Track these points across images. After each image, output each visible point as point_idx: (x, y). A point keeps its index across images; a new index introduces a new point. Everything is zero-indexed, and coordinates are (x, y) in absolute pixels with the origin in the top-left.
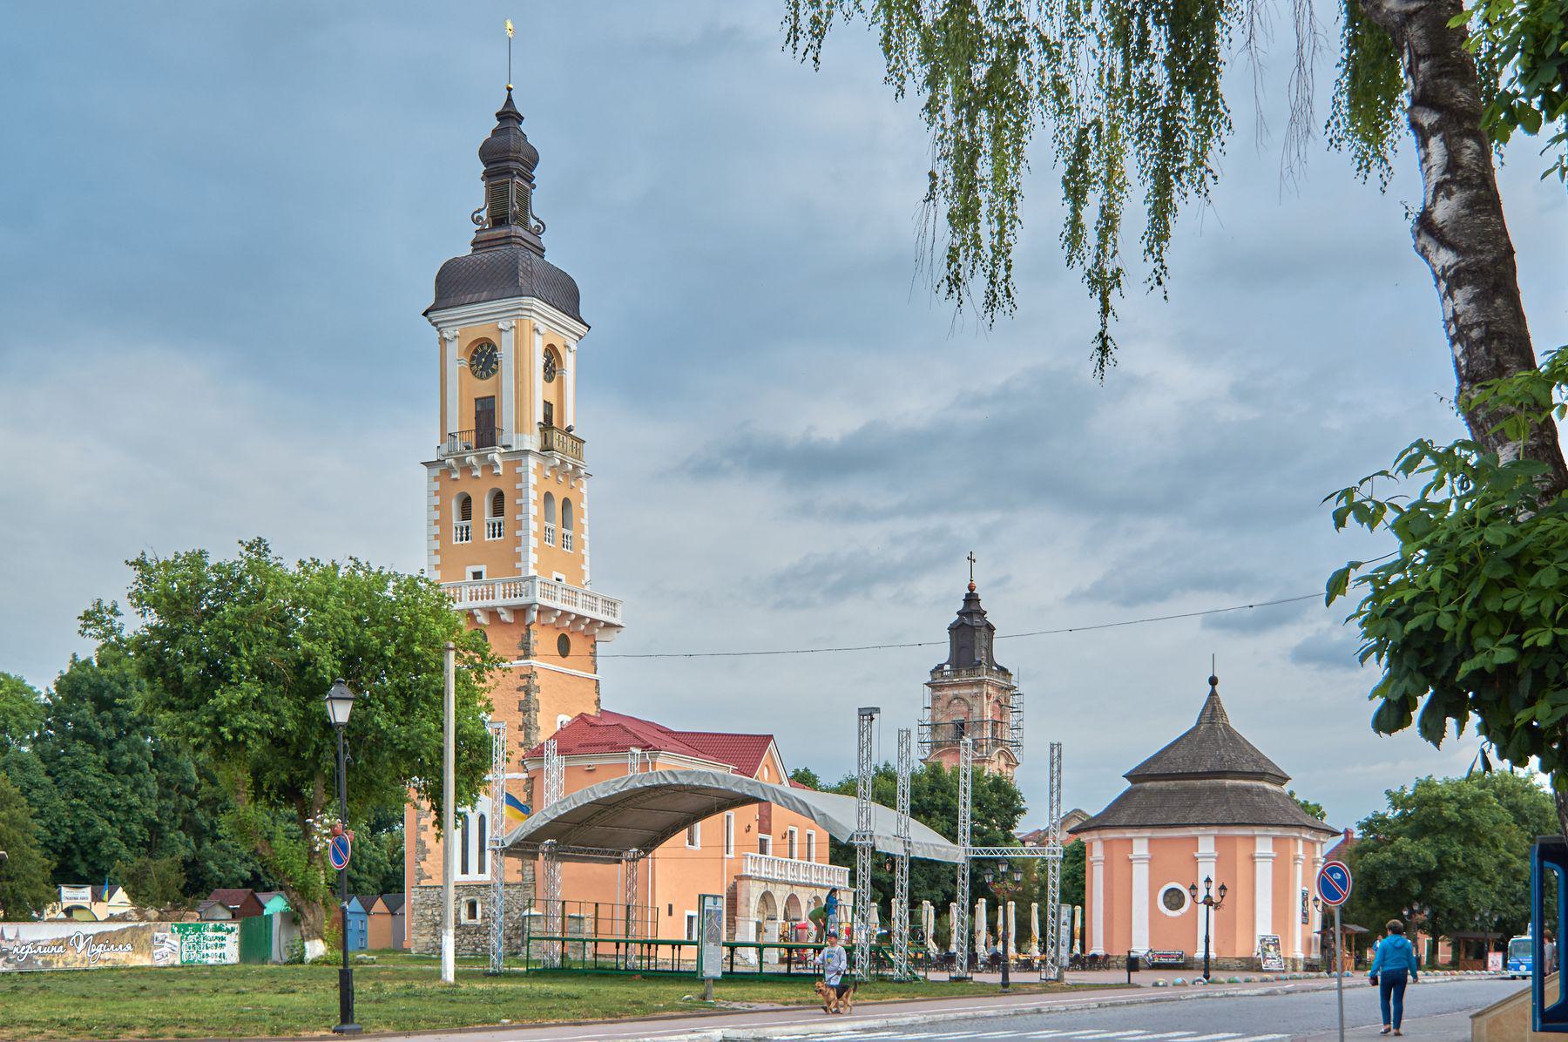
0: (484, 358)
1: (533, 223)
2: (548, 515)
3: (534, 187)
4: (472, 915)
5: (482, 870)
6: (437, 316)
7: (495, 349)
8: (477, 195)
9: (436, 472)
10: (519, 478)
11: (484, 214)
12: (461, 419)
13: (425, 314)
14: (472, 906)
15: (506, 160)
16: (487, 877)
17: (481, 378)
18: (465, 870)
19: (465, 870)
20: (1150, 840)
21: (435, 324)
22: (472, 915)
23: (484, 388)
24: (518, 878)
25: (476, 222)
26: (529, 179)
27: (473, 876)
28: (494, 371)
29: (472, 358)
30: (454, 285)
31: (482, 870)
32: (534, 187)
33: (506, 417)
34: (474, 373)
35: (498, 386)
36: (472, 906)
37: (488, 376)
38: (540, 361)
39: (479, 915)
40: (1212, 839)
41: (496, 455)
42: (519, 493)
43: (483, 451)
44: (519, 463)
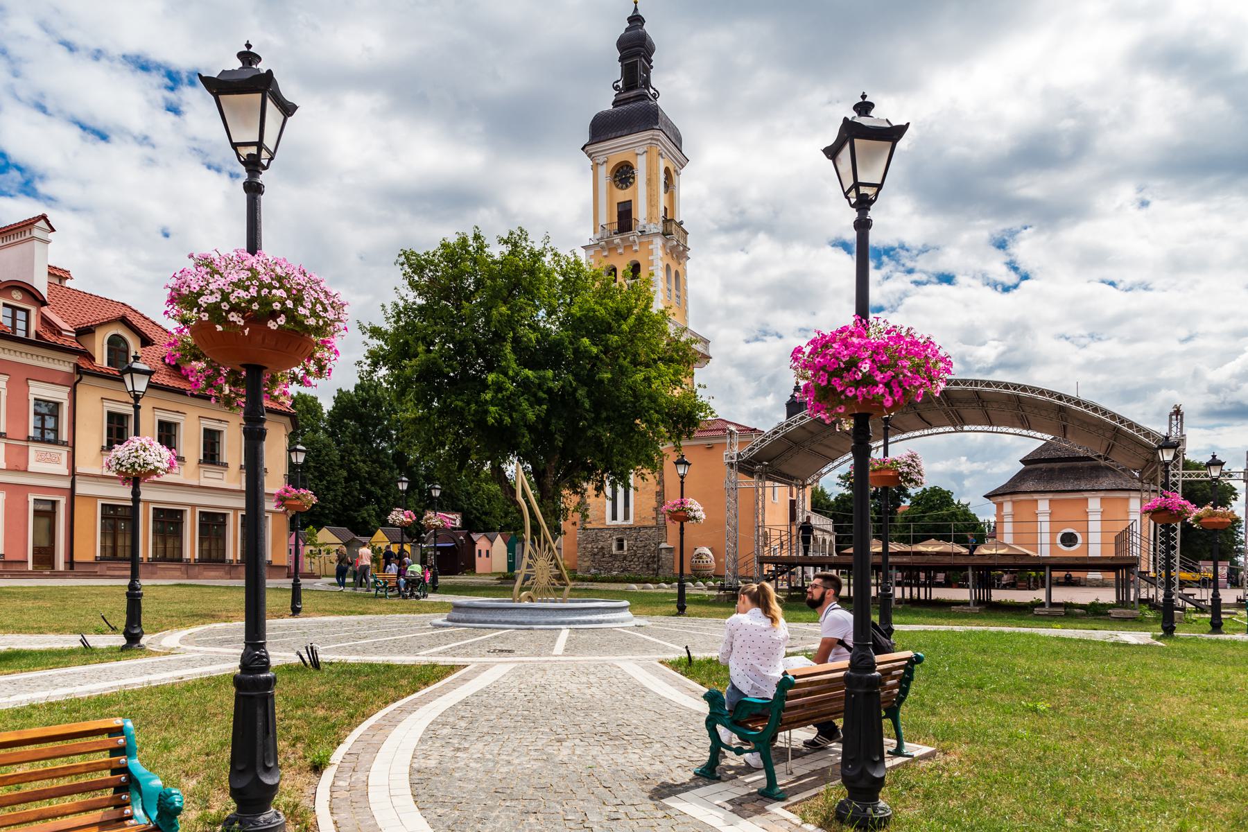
0: (623, 174)
1: (652, 91)
2: (668, 281)
4: (620, 547)
5: (626, 517)
7: (632, 168)
9: (591, 252)
10: (651, 252)
11: (620, 84)
12: (608, 216)
14: (620, 541)
15: (635, 50)
16: (631, 522)
18: (614, 517)
19: (614, 517)
20: (1050, 501)
21: (589, 156)
22: (620, 547)
23: (622, 195)
25: (615, 88)
26: (650, 61)
27: (620, 520)
30: (603, 128)
31: (626, 517)
33: (641, 213)
35: (635, 193)
36: (620, 541)
38: (662, 176)
39: (626, 548)
40: (1098, 500)
41: (632, 236)
42: (651, 263)
43: (626, 235)
44: (651, 243)
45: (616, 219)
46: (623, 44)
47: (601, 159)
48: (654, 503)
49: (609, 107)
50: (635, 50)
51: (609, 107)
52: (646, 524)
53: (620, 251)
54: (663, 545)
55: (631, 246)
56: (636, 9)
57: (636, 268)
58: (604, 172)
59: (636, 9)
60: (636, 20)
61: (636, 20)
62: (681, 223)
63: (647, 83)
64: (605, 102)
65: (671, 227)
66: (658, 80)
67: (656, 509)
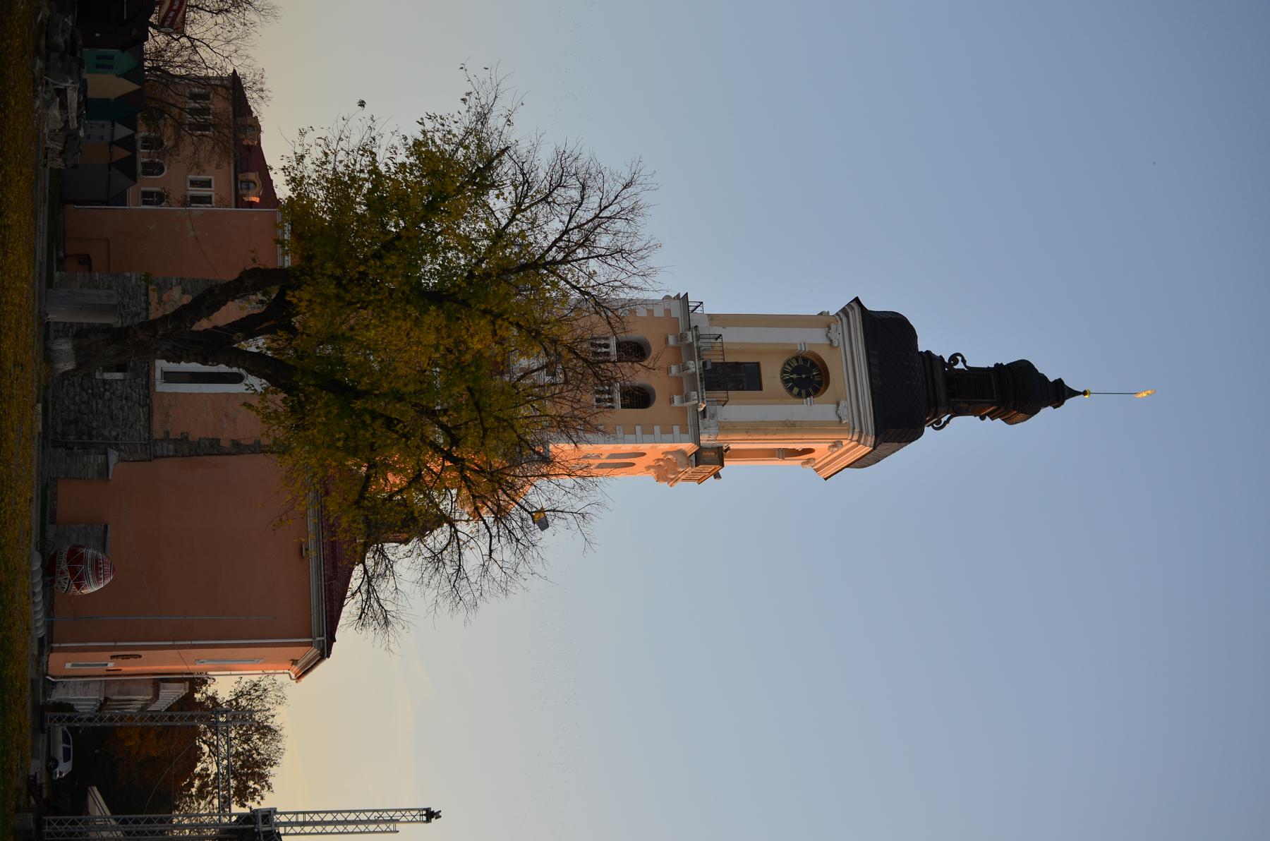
0: (807, 376)
3: (983, 418)
6: (856, 316)
8: (981, 357)
9: (676, 312)
10: (667, 430)
11: (960, 366)
13: (857, 300)
15: (1016, 391)
16: (162, 387)
17: (784, 372)
21: (844, 310)
23: (771, 374)
24: (158, 433)
25: (954, 358)
28: (790, 390)
29: (805, 360)
31: (170, 377)
32: (983, 418)
33: (738, 408)
34: (788, 363)
37: (785, 382)
42: (648, 431)
44: (684, 431)
45: (730, 359)
46: (1023, 368)
47: (837, 337)
48: (195, 435)
49: (922, 347)
50: (1016, 391)
51: (922, 347)
52: (157, 419)
53: (674, 369)
54: (113, 456)
55: (680, 392)
56: (1075, 393)
57: (639, 398)
58: (812, 340)
59: (1075, 393)
60: (1058, 393)
61: (1058, 393)
62: (717, 476)
63: (957, 412)
64: (933, 339)
65: (710, 459)
66: (964, 428)
67: (185, 438)
